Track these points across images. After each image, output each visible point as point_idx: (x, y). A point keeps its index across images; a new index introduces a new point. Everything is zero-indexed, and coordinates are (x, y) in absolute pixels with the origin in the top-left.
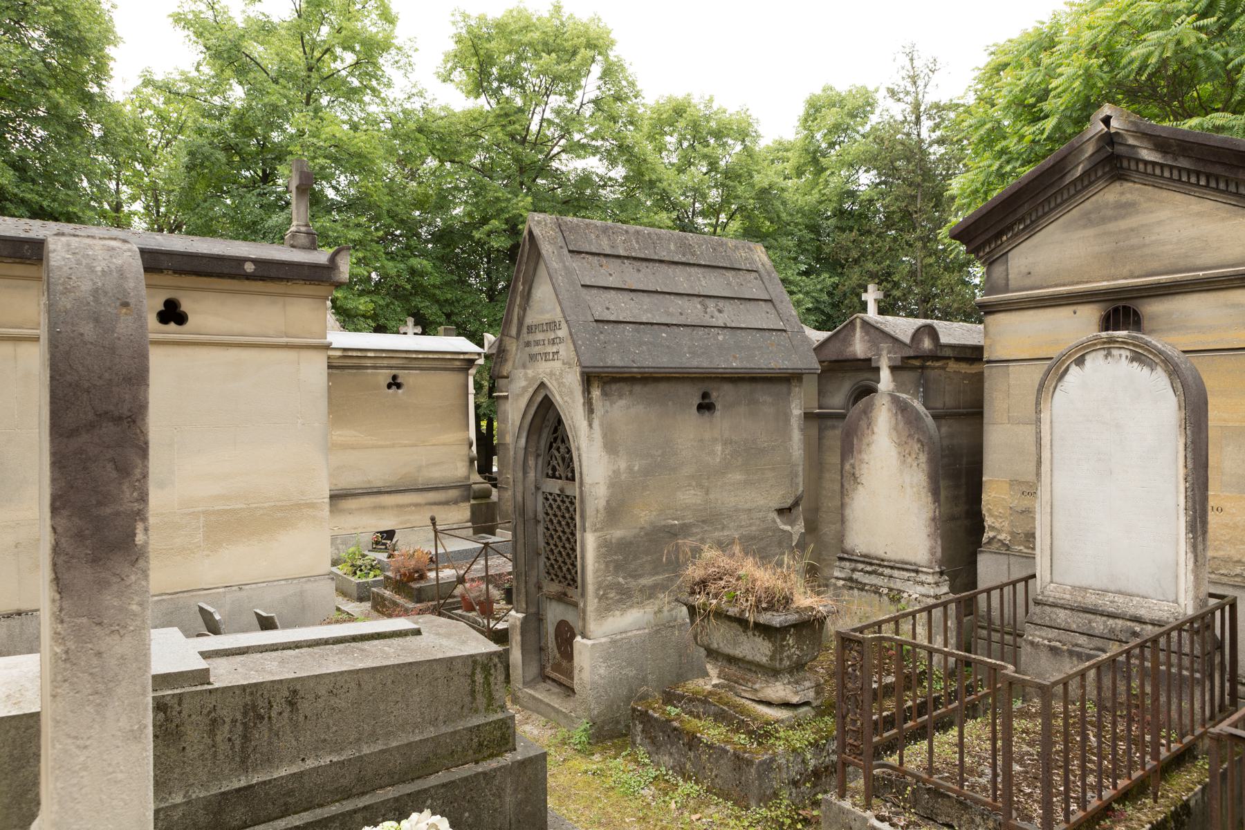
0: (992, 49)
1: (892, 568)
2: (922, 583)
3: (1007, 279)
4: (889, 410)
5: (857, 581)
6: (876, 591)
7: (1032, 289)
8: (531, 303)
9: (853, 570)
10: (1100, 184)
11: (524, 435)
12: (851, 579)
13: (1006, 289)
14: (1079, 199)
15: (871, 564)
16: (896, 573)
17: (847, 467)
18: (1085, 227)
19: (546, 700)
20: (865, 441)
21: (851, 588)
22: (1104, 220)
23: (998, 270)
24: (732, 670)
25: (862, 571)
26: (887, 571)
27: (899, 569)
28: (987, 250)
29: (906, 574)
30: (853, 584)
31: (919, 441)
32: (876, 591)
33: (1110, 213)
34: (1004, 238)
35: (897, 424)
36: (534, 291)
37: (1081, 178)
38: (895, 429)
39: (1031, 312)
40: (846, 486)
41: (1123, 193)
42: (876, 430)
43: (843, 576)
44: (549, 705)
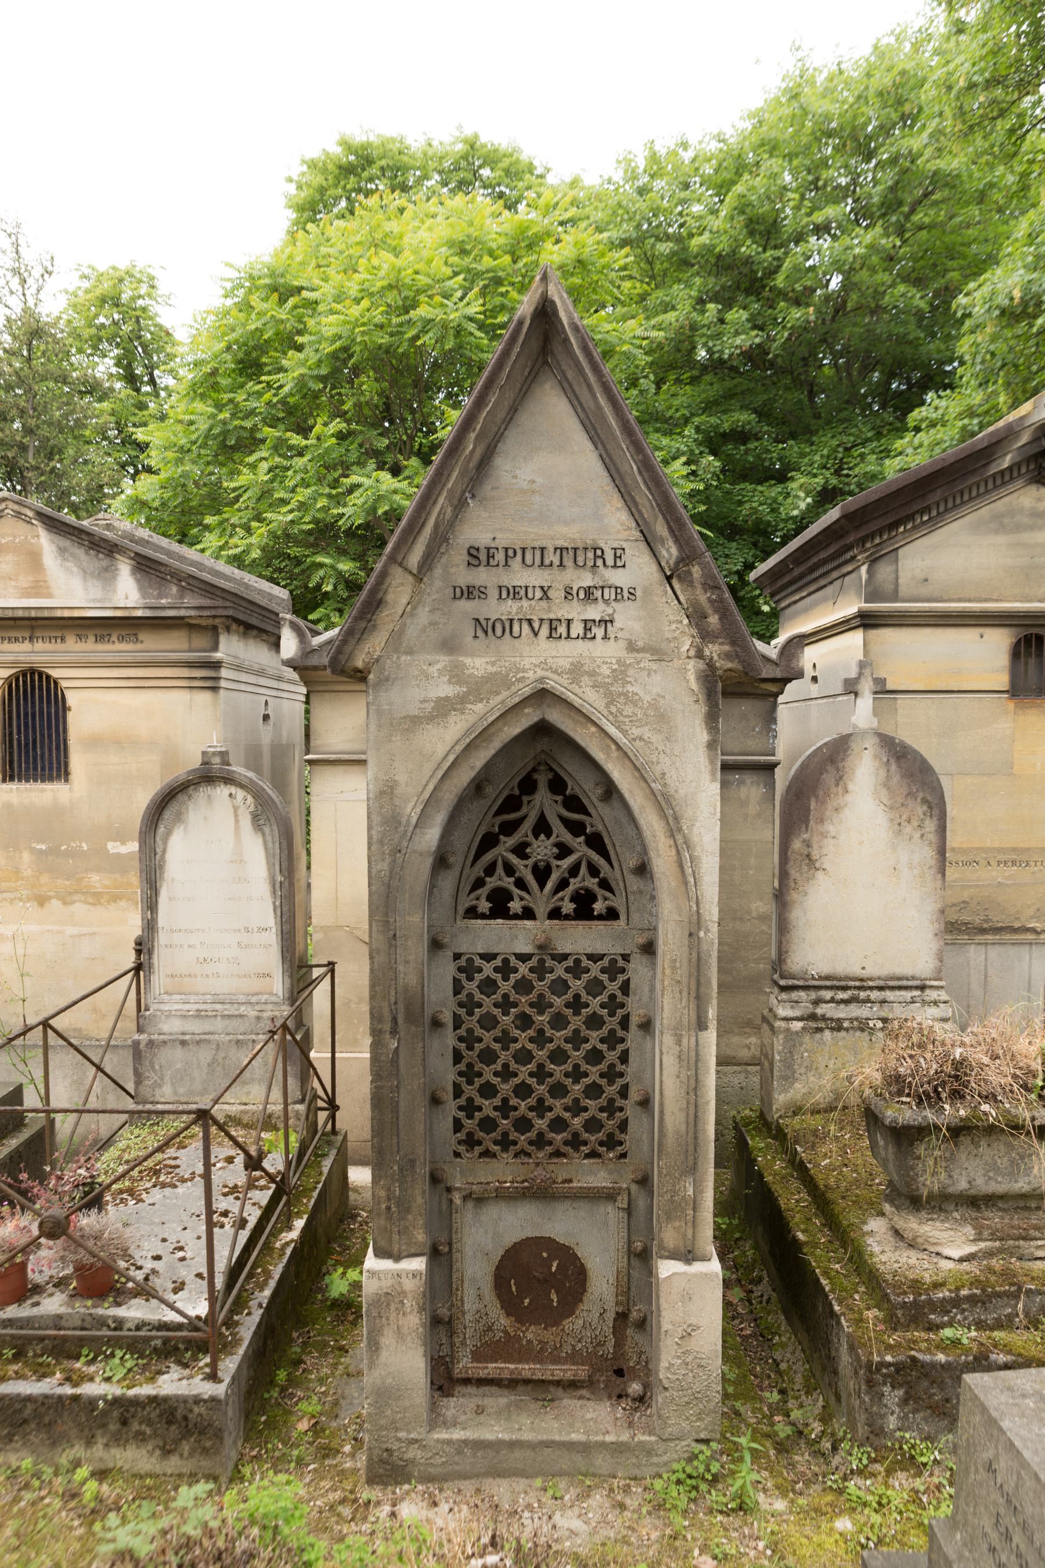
0: (86, 271)
1: (881, 988)
2: (936, 1003)
3: (897, 585)
4: (876, 757)
5: (824, 1018)
6: (862, 1026)
7: (928, 601)
8: (486, 489)
9: (817, 1002)
10: (1020, 483)
11: (439, 819)
12: (813, 1017)
13: (895, 597)
14: (994, 496)
15: (845, 988)
16: (889, 995)
17: (797, 845)
18: (996, 532)
19: (527, 1436)
20: (831, 804)
21: (819, 1030)
22: (1018, 528)
23: (884, 570)
24: (995, 1219)
25: (832, 1000)
26: (875, 995)
27: (892, 988)
28: (877, 541)
29: (908, 995)
30: (815, 1022)
31: (924, 801)
32: (862, 1026)
33: (1025, 520)
34: (902, 529)
35: (888, 777)
36: (498, 461)
37: (1010, 468)
38: (886, 785)
39: (927, 631)
40: (794, 873)
41: (1039, 500)
42: (851, 786)
43: (797, 1013)
44: (513, 1445)
